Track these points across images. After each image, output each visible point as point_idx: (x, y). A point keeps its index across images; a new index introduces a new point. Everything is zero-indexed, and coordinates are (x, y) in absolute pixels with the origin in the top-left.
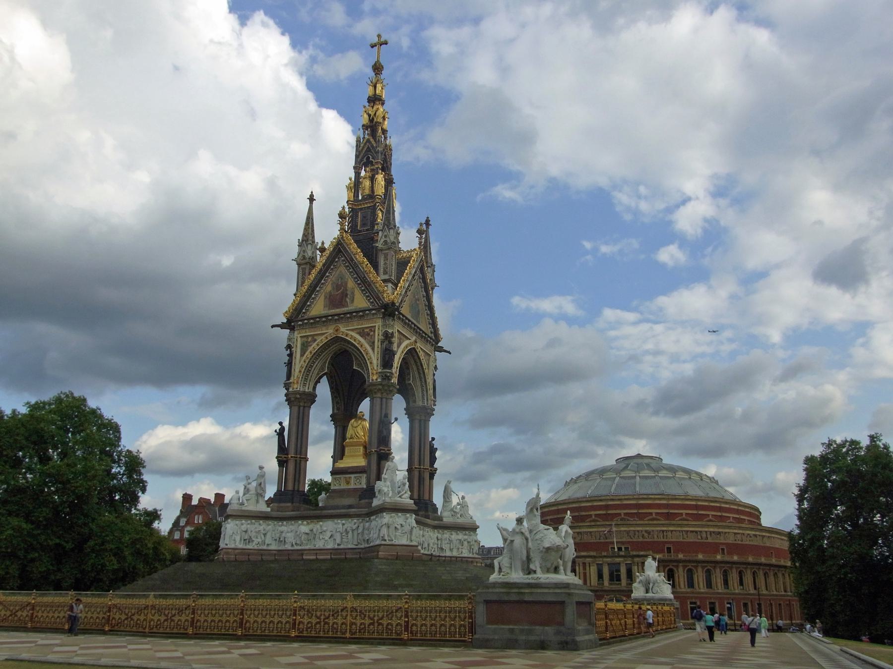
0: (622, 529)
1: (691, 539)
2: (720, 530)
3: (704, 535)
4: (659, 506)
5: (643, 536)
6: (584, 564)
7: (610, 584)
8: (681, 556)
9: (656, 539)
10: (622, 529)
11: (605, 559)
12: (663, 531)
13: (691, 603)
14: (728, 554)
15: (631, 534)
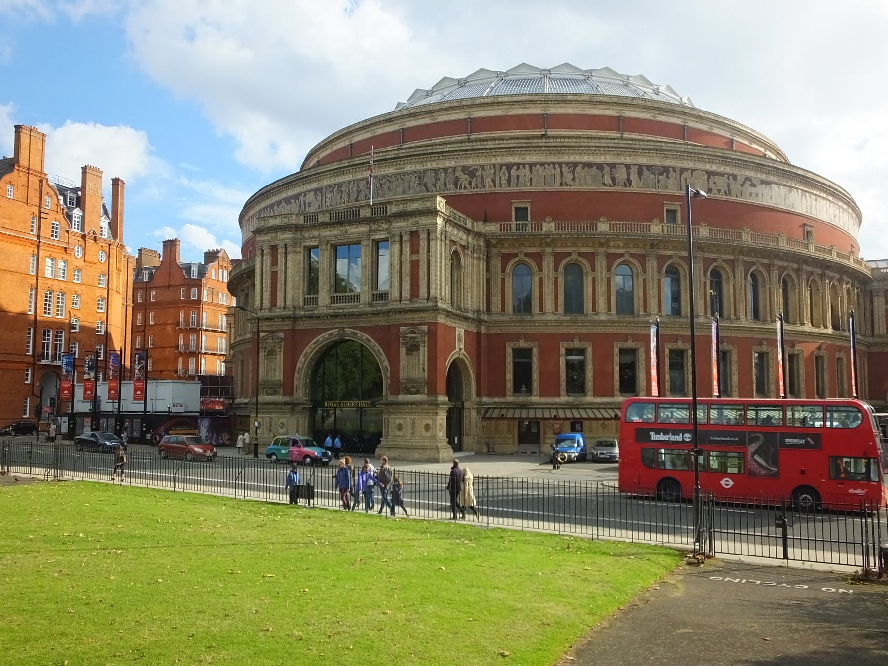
0: (409, 168)
1: (585, 183)
2: (668, 163)
3: (621, 175)
4: (521, 122)
5: (457, 179)
6: (274, 248)
7: (334, 300)
8: (548, 226)
9: (487, 190)
10: (409, 168)
11: (326, 233)
12: (509, 166)
13: (569, 352)
14: (686, 221)
15: (429, 179)
